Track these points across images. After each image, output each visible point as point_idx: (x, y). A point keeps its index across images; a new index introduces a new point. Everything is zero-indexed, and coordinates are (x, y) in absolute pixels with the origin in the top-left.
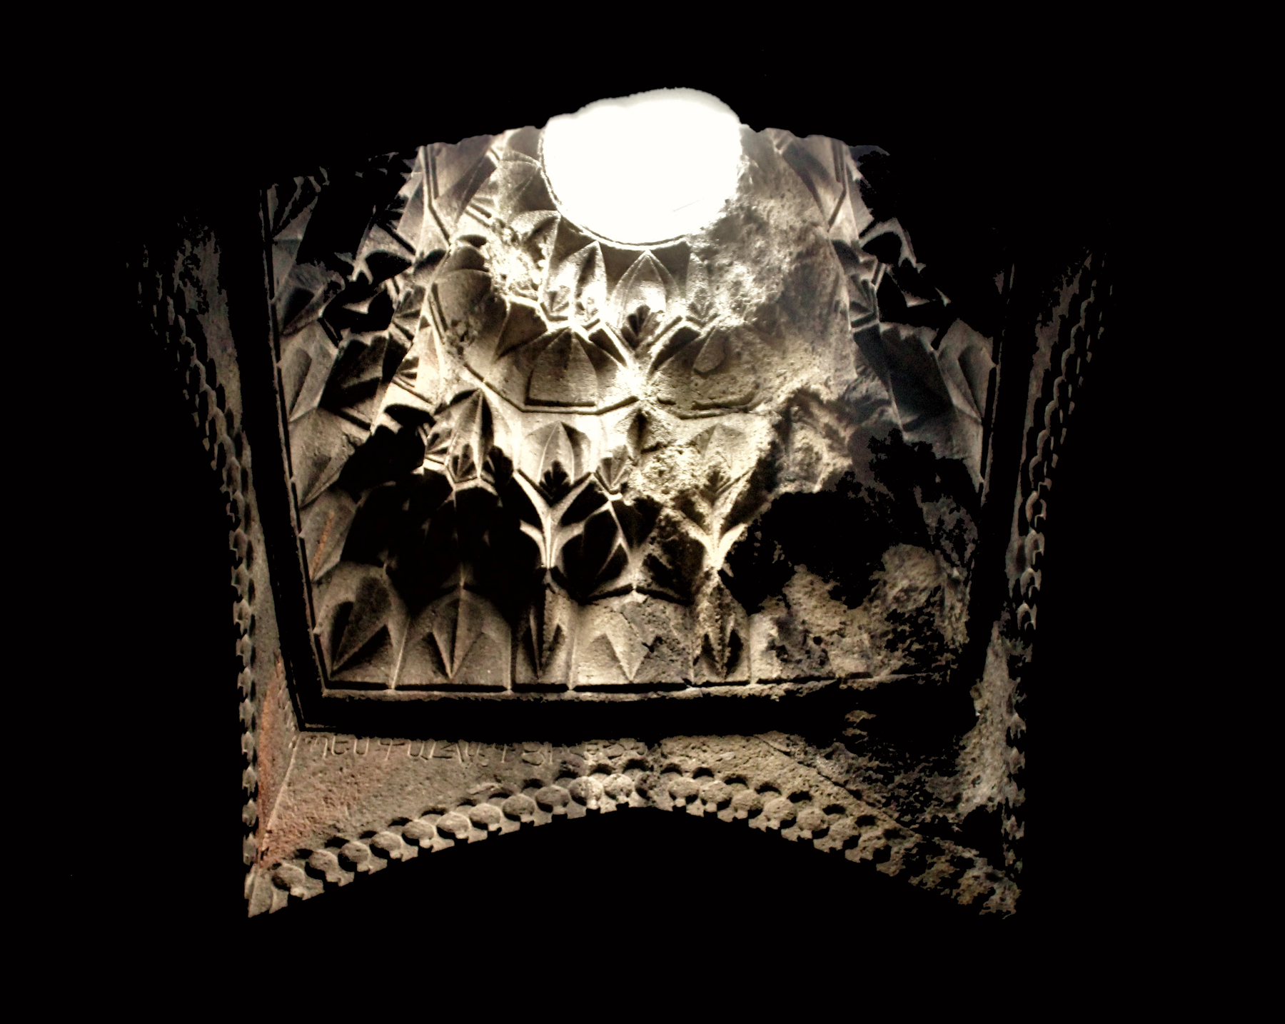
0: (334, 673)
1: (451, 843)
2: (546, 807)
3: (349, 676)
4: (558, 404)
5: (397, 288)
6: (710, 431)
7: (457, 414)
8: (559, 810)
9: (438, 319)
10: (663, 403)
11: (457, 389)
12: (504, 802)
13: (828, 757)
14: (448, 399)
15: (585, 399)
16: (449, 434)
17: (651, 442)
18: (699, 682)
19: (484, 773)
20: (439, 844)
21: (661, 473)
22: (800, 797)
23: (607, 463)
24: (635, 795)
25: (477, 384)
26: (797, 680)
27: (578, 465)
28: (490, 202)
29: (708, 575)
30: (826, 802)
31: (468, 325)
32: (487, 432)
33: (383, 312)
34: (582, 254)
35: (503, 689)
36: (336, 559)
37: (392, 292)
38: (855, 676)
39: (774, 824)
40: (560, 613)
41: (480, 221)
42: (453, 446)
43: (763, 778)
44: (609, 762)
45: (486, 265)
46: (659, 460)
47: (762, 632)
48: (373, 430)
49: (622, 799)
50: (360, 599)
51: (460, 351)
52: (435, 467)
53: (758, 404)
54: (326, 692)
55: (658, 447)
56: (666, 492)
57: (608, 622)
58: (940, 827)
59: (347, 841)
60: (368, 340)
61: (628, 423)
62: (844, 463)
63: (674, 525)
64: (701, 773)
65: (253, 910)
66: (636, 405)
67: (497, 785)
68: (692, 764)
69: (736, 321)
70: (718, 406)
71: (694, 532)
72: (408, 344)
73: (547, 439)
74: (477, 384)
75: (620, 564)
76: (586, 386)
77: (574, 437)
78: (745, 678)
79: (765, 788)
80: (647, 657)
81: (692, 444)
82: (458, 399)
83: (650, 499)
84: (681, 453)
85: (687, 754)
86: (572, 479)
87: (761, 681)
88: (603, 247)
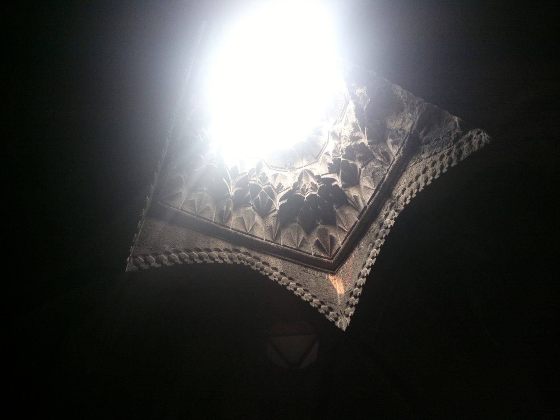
0: (330, 256)
1: (370, 269)
3: (333, 253)
6: (346, 117)
11: (298, 176)
12: (374, 247)
13: (423, 153)
14: (297, 180)
16: (305, 185)
17: (338, 135)
18: (386, 172)
19: (367, 245)
22: (424, 171)
23: (334, 151)
24: (396, 213)
26: (402, 145)
30: (430, 164)
32: (312, 174)
37: (254, 182)
38: (412, 127)
40: (353, 192)
42: (309, 186)
43: (414, 176)
50: (320, 237)
51: (293, 168)
55: (340, 134)
57: (365, 182)
58: (458, 137)
63: (356, 145)
65: (344, 328)
68: (400, 191)
71: (359, 142)
72: (270, 185)
73: (324, 160)
74: (302, 169)
75: (355, 166)
80: (374, 180)
81: (345, 124)
83: (347, 147)
85: (398, 191)
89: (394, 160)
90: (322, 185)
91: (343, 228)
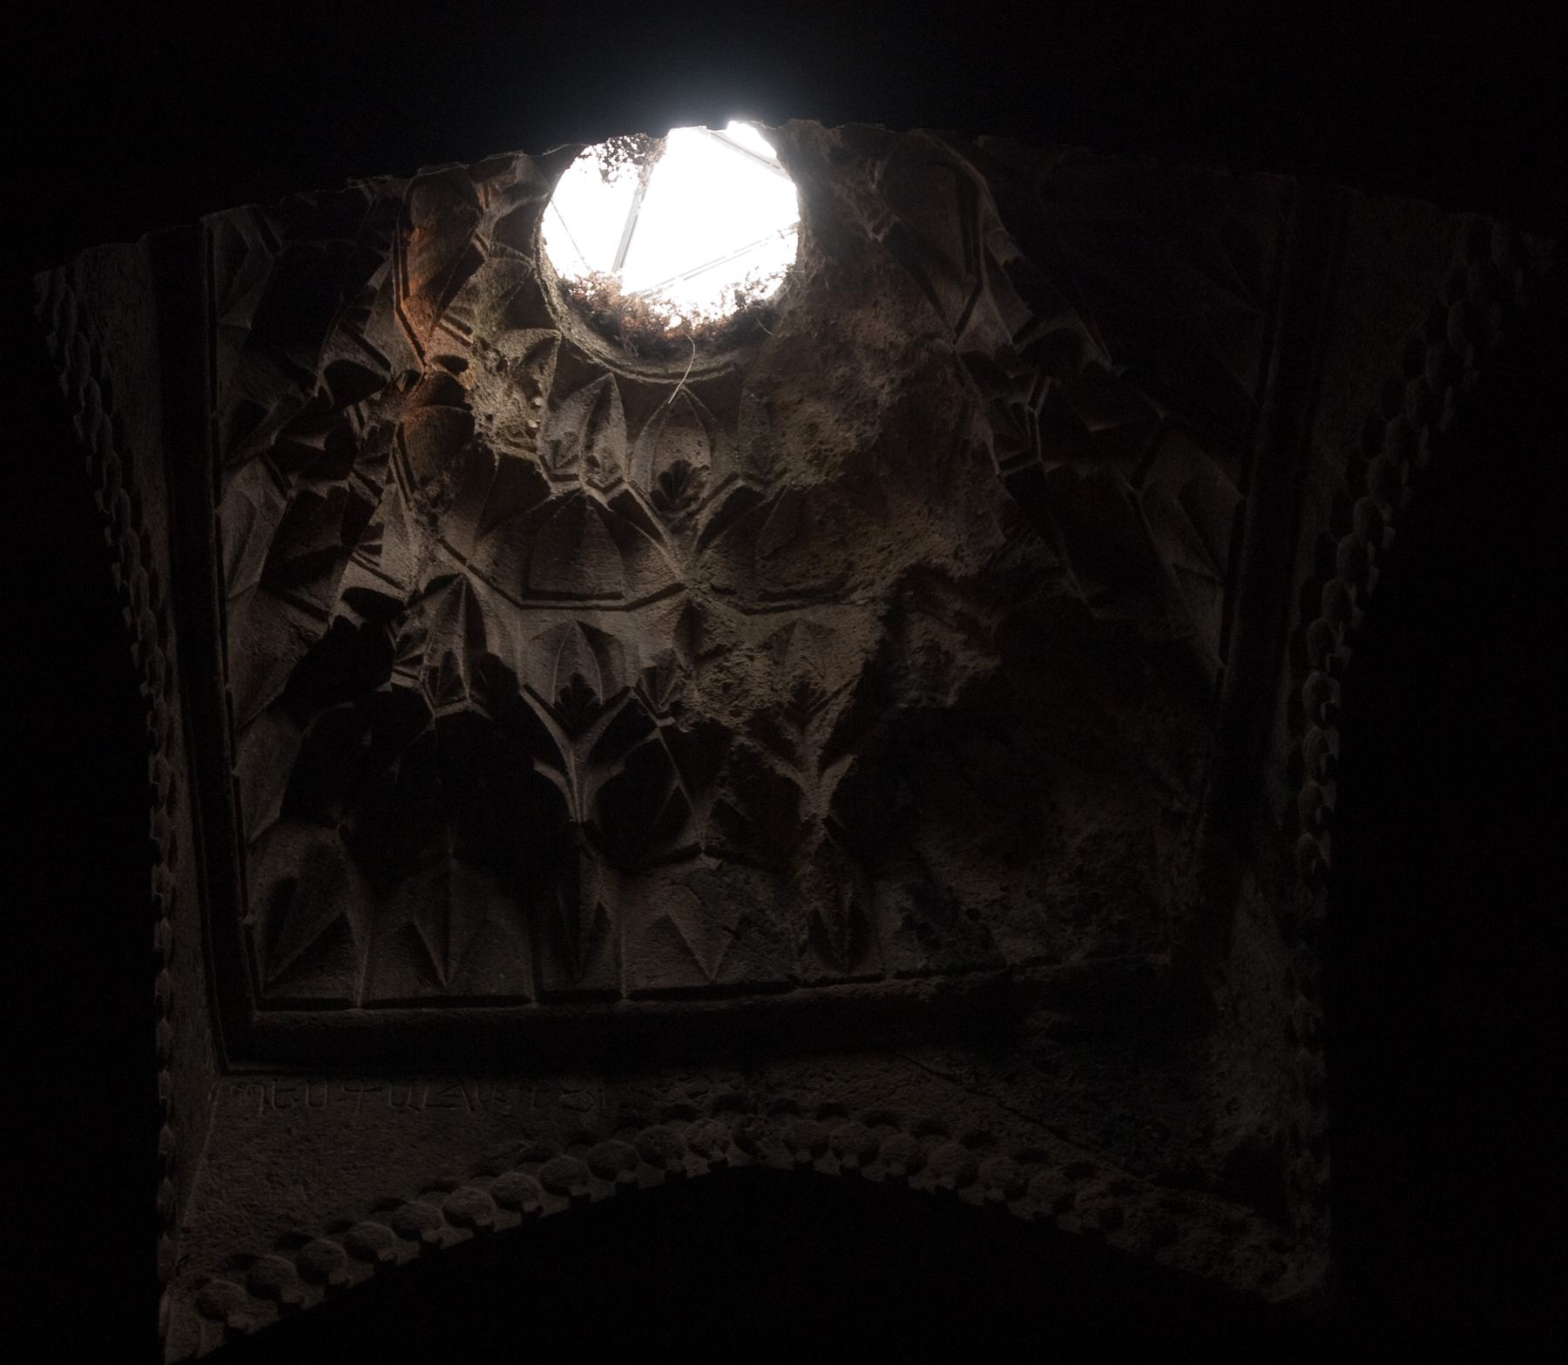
1: (469, 1234)
2: (606, 1174)
4: (570, 596)
5: (361, 418)
6: (789, 629)
7: (432, 608)
8: (625, 1176)
9: (403, 475)
10: (720, 592)
11: (431, 572)
12: (541, 1167)
15: (607, 589)
16: (423, 635)
17: (708, 645)
20: (451, 1236)
21: (726, 687)
23: (651, 674)
24: (733, 1147)
25: (458, 566)
27: (608, 679)
28: (469, 313)
29: (809, 827)
31: (443, 486)
32: (476, 636)
33: (345, 452)
34: (592, 390)
35: (521, 1000)
36: (275, 812)
39: (947, 1182)
40: (600, 891)
41: (457, 338)
44: (689, 1101)
45: (468, 401)
46: (721, 669)
47: (893, 905)
48: (331, 621)
49: (717, 1154)
51: (433, 520)
52: (407, 683)
53: (854, 589)
54: (257, 1015)
55: (719, 651)
56: (736, 713)
57: (666, 900)
59: (307, 1239)
60: (323, 490)
61: (674, 620)
62: (989, 664)
64: (827, 1112)
66: (683, 595)
67: (528, 1144)
69: (811, 478)
70: (798, 595)
71: (782, 769)
72: (375, 502)
73: (559, 643)
74: (458, 566)
76: (604, 572)
77: (598, 641)
78: (878, 971)
79: (927, 1129)
81: (766, 646)
82: (437, 585)
84: (751, 658)
86: (601, 698)
87: (901, 975)
88: (619, 378)
89: (878, 978)
90: (478, 709)
91: (435, 956)
